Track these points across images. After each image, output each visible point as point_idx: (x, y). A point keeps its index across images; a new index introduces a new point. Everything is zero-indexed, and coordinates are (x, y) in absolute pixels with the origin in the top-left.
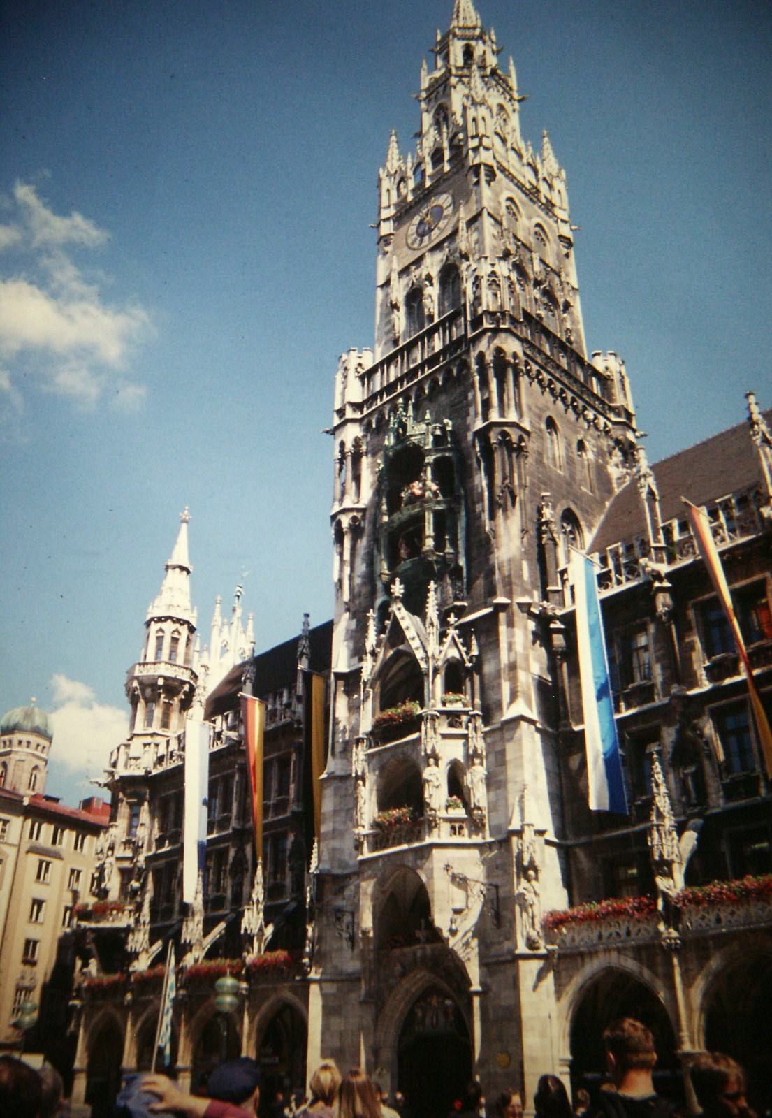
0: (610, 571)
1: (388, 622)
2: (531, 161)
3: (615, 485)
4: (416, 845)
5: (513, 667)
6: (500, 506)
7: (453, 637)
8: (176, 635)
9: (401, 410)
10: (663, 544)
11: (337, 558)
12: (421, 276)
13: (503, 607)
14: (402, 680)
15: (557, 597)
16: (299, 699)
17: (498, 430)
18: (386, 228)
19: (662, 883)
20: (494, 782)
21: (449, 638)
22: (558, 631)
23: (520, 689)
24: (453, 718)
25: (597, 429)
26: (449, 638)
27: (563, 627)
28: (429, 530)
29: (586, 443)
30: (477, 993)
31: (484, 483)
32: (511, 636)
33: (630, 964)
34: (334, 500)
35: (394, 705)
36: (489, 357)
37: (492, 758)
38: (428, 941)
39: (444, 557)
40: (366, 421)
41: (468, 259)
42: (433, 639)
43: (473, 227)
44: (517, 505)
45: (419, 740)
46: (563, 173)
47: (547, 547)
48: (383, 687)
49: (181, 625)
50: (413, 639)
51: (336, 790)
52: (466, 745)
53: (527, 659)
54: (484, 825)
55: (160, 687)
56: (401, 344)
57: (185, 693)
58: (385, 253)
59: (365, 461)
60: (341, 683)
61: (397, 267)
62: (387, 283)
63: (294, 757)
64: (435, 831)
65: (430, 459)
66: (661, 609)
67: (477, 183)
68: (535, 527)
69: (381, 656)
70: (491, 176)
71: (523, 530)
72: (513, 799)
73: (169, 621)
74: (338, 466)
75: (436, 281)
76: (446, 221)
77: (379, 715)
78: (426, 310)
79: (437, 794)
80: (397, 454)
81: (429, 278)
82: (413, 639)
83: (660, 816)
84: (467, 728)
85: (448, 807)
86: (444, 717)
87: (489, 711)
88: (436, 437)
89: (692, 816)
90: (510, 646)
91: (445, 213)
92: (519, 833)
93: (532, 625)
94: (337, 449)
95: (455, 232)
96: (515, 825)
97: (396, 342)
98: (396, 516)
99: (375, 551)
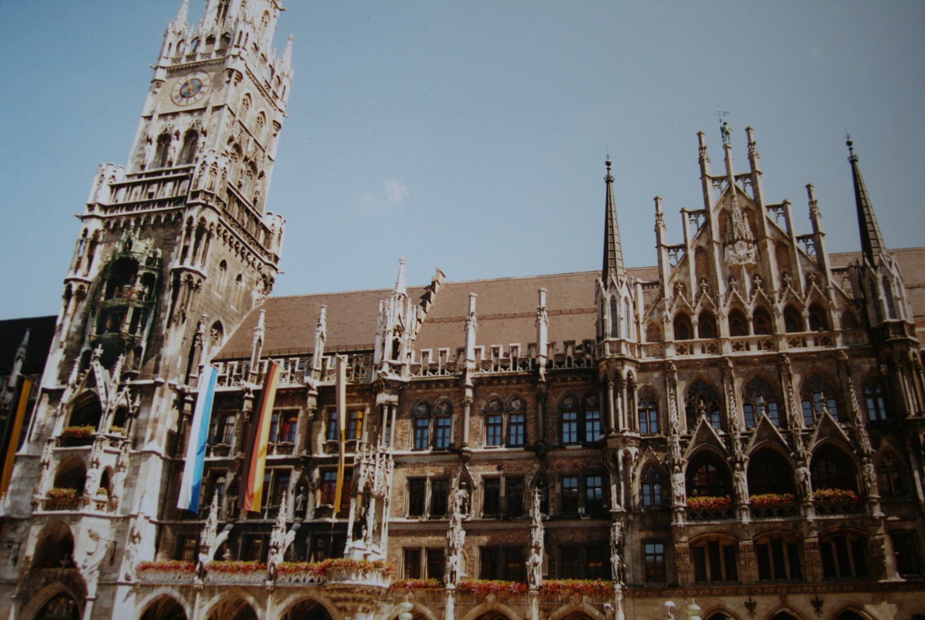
1: (88, 371)
3: (254, 304)
4: (74, 512)
5: (156, 421)
10: (257, 372)
14: (87, 411)
16: (10, 389)
19: (202, 557)
20: (128, 483)
22: (189, 402)
24: (114, 441)
25: (253, 266)
28: (129, 319)
29: (243, 277)
30: (91, 600)
31: (169, 303)
33: (176, 594)
34: (71, 268)
36: (195, 223)
37: (131, 469)
38: (67, 566)
39: (133, 338)
45: (90, 450)
48: (74, 409)
51: (26, 464)
53: (165, 417)
54: (116, 506)
59: (99, 249)
64: (87, 507)
65: (141, 272)
66: (245, 409)
68: (193, 334)
69: (77, 391)
72: (137, 496)
77: (67, 428)
80: (121, 259)
83: (210, 522)
85: (98, 493)
88: (149, 258)
89: (229, 522)
90: (158, 408)
92: (136, 517)
96: (134, 512)
98: (109, 302)
99: (90, 315)
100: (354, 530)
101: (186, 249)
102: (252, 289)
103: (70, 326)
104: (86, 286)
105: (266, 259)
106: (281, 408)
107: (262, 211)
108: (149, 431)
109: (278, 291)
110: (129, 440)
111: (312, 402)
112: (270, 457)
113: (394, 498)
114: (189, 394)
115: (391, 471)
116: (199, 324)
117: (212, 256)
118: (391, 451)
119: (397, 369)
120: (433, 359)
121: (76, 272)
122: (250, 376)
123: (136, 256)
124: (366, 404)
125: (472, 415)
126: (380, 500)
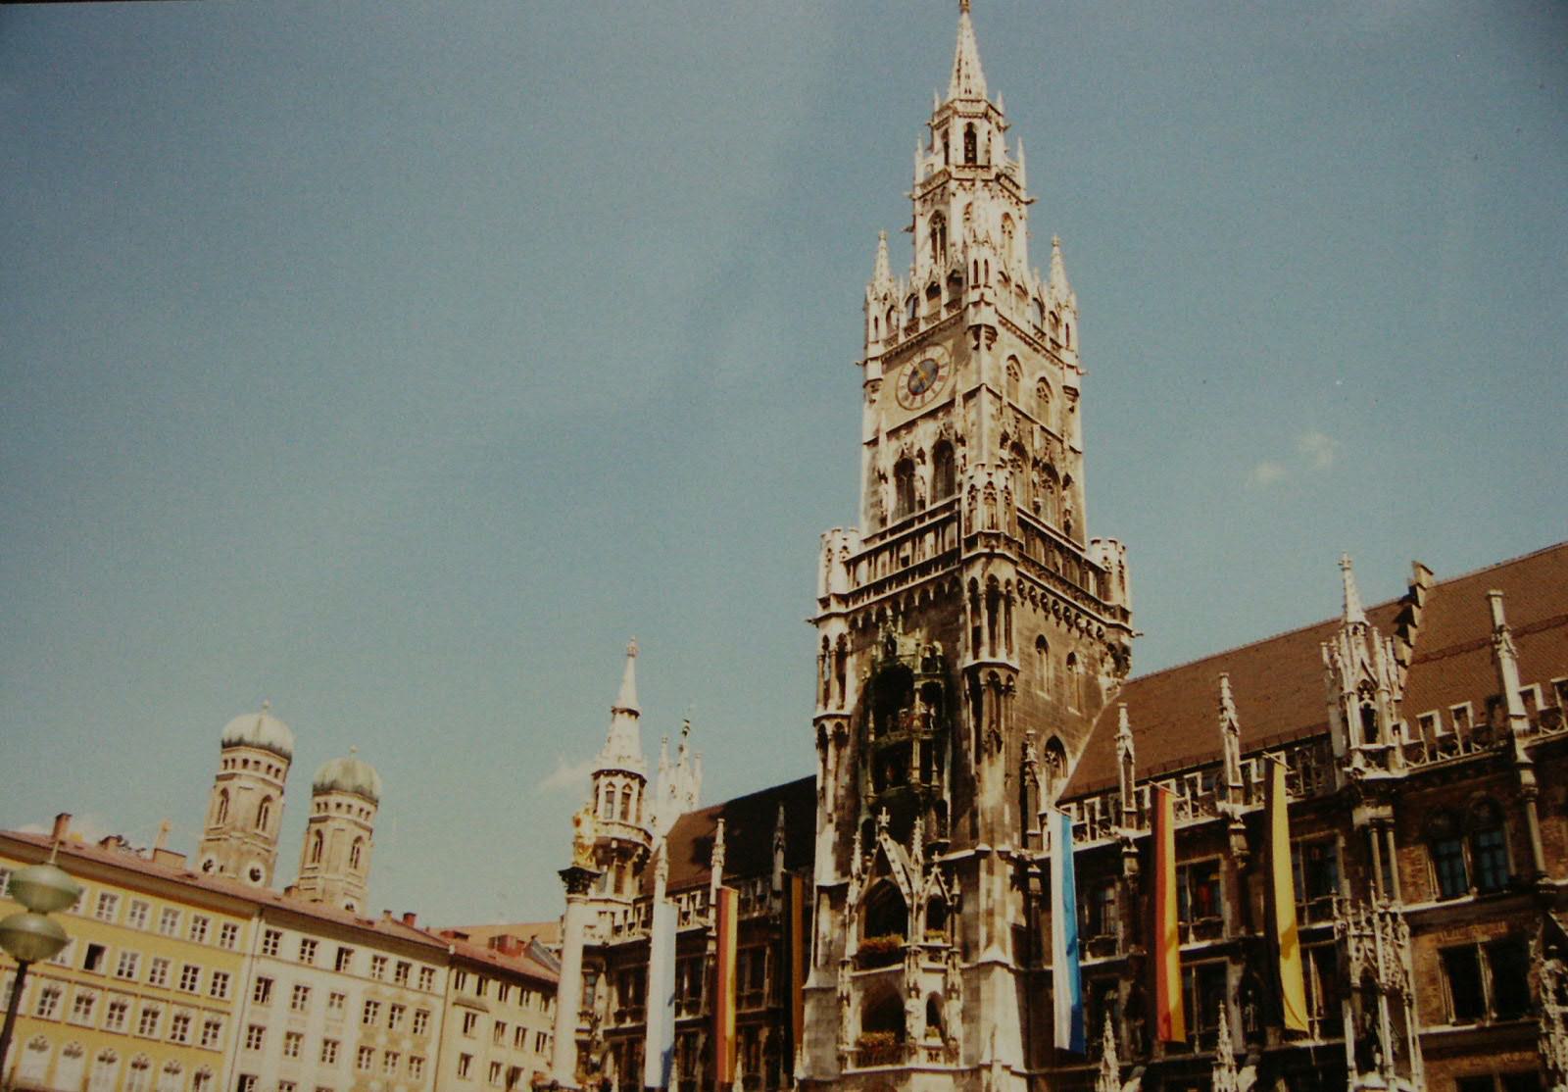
0: (1085, 825)
1: (874, 851)
2: (1037, 296)
3: (1104, 697)
5: (990, 913)
6: (986, 750)
7: (936, 876)
8: (627, 791)
10: (1133, 809)
12: (912, 445)
14: (885, 911)
16: (776, 895)
17: (988, 670)
18: (875, 370)
20: (969, 1016)
21: (933, 875)
22: (1034, 875)
25: (1090, 635)
26: (933, 875)
28: (916, 763)
31: (972, 724)
32: (992, 883)
34: (818, 701)
36: (982, 588)
37: (968, 993)
40: (851, 617)
41: (964, 444)
43: (971, 403)
44: (1003, 750)
45: (902, 971)
46: (1073, 298)
47: (1029, 789)
49: (633, 779)
52: (945, 979)
53: (1004, 904)
55: (613, 850)
56: (890, 525)
57: (638, 856)
58: (873, 401)
59: (851, 662)
61: (886, 427)
62: (874, 442)
63: (768, 952)
65: (918, 685)
66: (1127, 873)
67: (977, 348)
68: (1018, 765)
69: (866, 883)
70: (993, 334)
73: (620, 776)
75: (928, 458)
76: (941, 383)
78: (917, 494)
79: (917, 1023)
81: (921, 454)
84: (947, 963)
87: (968, 949)
88: (924, 659)
91: (941, 372)
94: (821, 643)
95: (951, 403)
97: (883, 521)
98: (883, 739)
99: (860, 765)
100: (1357, 1057)
101: (977, 631)
102: (1096, 672)
103: (836, 789)
104: (845, 722)
105: (1107, 619)
106: (1187, 862)
107: (1082, 543)
108: (983, 931)
109: (1141, 666)
110: (955, 949)
111: (1237, 843)
112: (1185, 947)
113: (1420, 990)
114: (1033, 862)
115: (1406, 942)
116: (1024, 748)
117: (1020, 633)
118: (1399, 907)
119: (1381, 758)
120: (1444, 728)
121: (826, 705)
122: (1124, 817)
123: (905, 661)
124: (1336, 831)
125: (1541, 817)
126: (1396, 998)
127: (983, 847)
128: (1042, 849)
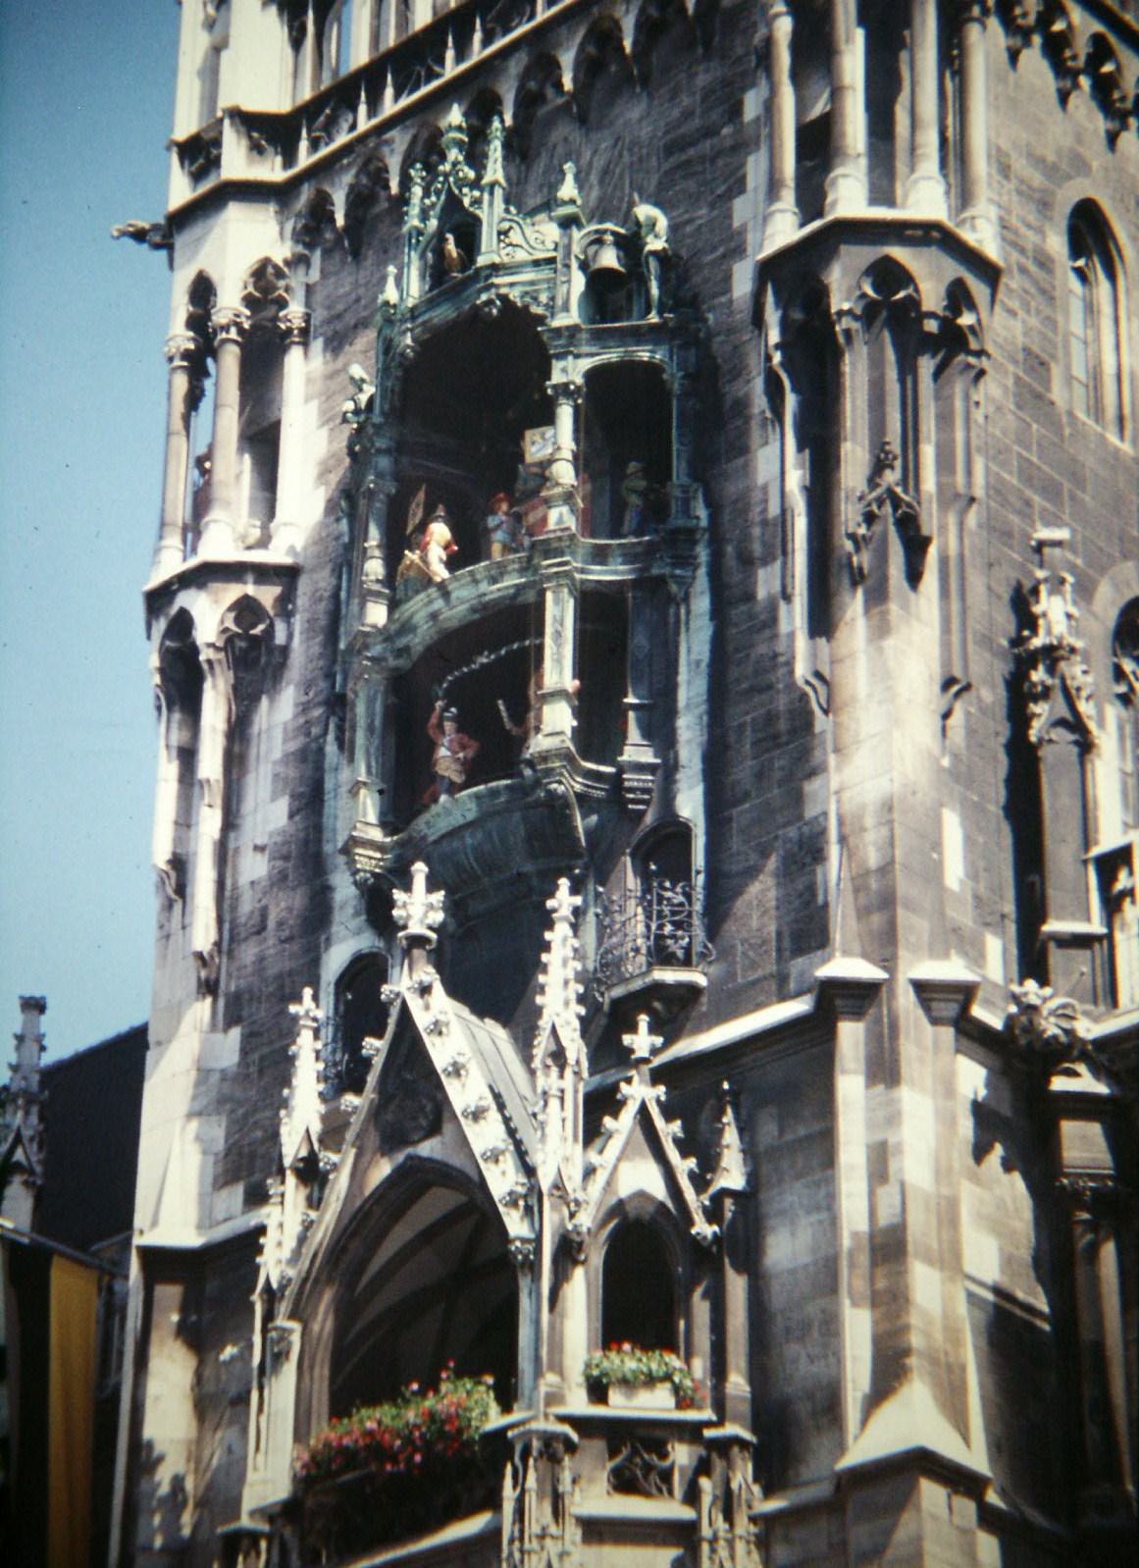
1: (375, 1046)
5: (889, 1247)
6: (857, 578)
7: (643, 1110)
9: (454, 154)
11: (169, 770)
13: (859, 996)
15: (1082, 963)
21: (628, 1114)
22: (1082, 1106)
23: (916, 1340)
24: (633, 1452)
26: (628, 1114)
27: (1102, 1089)
28: (559, 670)
31: (796, 478)
35: (392, 1393)
39: (616, 782)
40: (306, 193)
42: (561, 1121)
48: (346, 1312)
50: (477, 1115)
53: (948, 1215)
59: (300, 369)
60: (169, 1294)
65: (570, 371)
68: (1002, 668)
69: (341, 1183)
71: (948, 683)
74: (181, 383)
77: (324, 1431)
80: (434, 343)
82: (477, 1115)
84: (692, 1497)
86: (598, 1445)
88: (600, 283)
93: (972, 1078)
94: (181, 308)
99: (331, 748)
108: (858, 1329)
110: (731, 1429)
116: (1022, 606)
123: (512, 287)
127: (845, 965)
128: (1115, 1003)
